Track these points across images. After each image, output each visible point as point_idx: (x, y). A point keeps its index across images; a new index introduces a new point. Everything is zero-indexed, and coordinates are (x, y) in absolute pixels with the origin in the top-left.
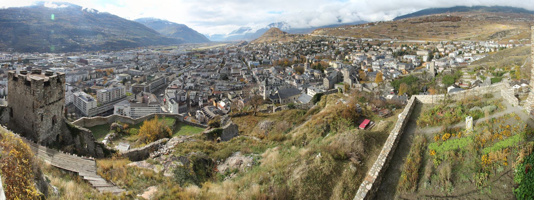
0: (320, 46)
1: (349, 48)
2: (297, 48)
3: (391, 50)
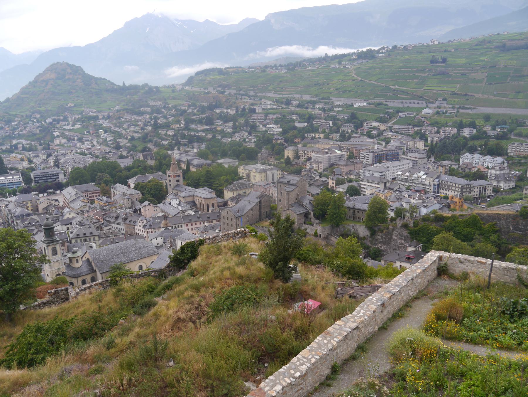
0: (209, 121)
1: (295, 128)
2: (142, 129)
3: (423, 137)
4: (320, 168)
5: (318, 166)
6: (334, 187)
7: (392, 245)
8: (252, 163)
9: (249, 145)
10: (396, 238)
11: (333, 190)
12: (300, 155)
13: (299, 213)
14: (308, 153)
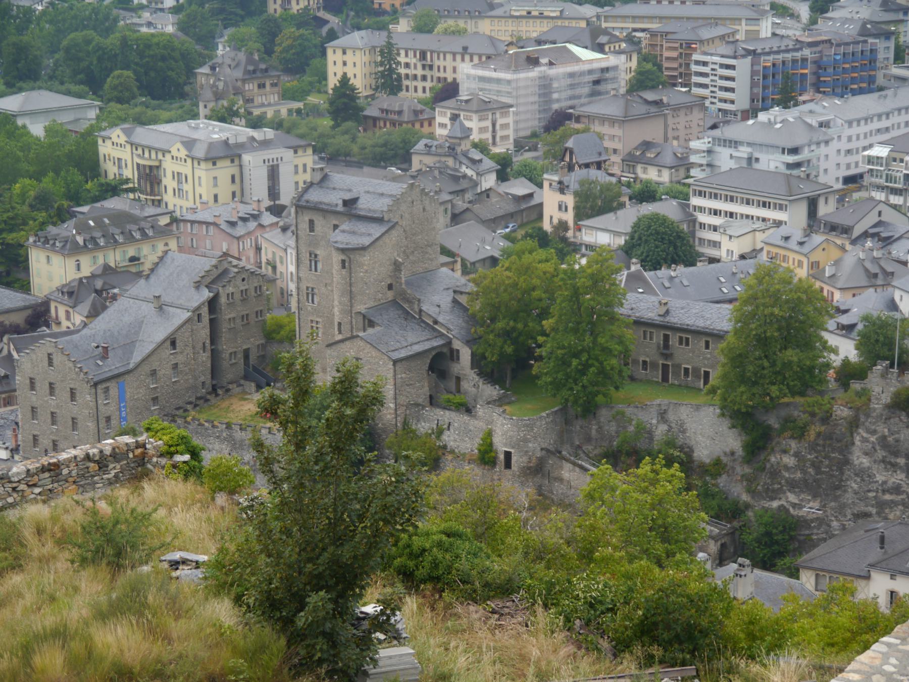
4: (499, 133)
5: (488, 123)
6: (571, 223)
7: (849, 497)
8: (165, 115)
9: (149, 24)
10: (865, 461)
11: (564, 240)
12: (403, 71)
13: (403, 354)
14: (441, 63)
